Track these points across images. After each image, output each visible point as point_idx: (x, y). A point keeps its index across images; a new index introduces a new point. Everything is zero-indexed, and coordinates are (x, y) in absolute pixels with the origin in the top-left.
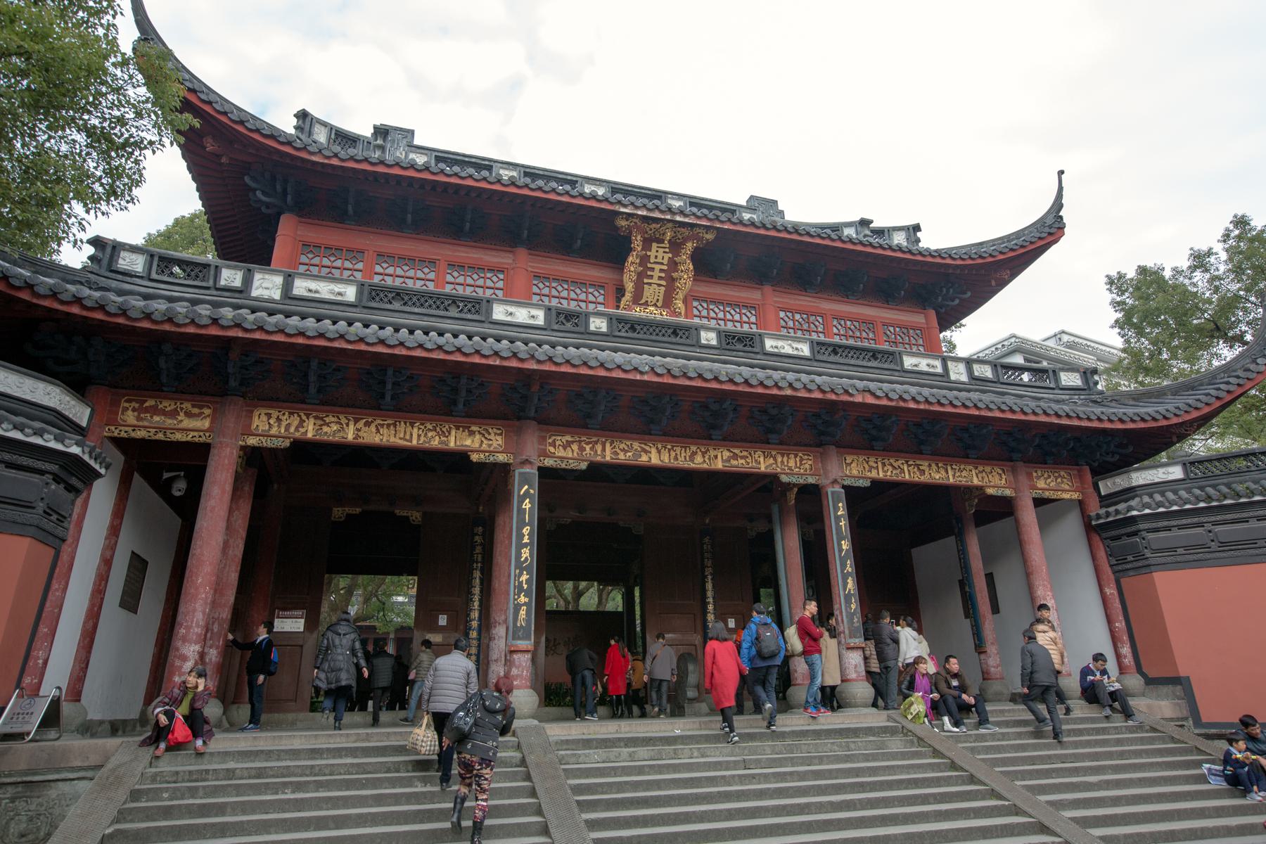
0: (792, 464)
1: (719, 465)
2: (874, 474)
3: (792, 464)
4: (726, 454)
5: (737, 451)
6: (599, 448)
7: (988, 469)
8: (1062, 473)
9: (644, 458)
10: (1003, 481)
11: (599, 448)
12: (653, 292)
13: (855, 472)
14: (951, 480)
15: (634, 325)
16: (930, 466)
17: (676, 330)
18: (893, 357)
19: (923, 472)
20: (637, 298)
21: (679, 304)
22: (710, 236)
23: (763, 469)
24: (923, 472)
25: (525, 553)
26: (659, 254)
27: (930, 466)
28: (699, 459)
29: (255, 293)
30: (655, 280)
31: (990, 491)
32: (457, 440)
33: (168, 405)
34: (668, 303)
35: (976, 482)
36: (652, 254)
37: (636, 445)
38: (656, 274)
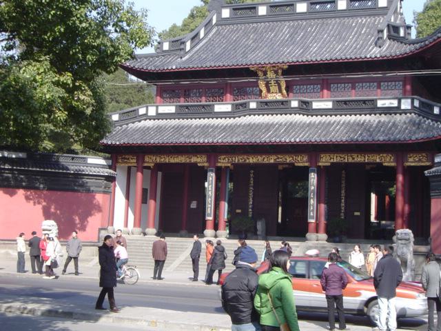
0: (299, 159)
1: (272, 161)
2: (332, 161)
3: (299, 159)
4: (276, 157)
5: (279, 156)
6: (234, 159)
7: (384, 155)
8: (424, 154)
9: (247, 161)
10: (392, 160)
11: (234, 159)
12: (274, 88)
13: (324, 160)
14: (366, 161)
15: (266, 103)
16: (358, 156)
17: (282, 103)
18: (374, 102)
19: (353, 159)
20: (268, 91)
21: (284, 91)
22: (287, 67)
23: (288, 161)
24: (353, 159)
25: (210, 193)
26: (271, 75)
27: (358, 156)
28: (266, 160)
29: (149, 114)
30: (273, 84)
31: (384, 164)
32: (194, 160)
33: (127, 157)
34: (280, 91)
35: (378, 160)
36: (268, 76)
37: (245, 157)
38: (272, 82)
